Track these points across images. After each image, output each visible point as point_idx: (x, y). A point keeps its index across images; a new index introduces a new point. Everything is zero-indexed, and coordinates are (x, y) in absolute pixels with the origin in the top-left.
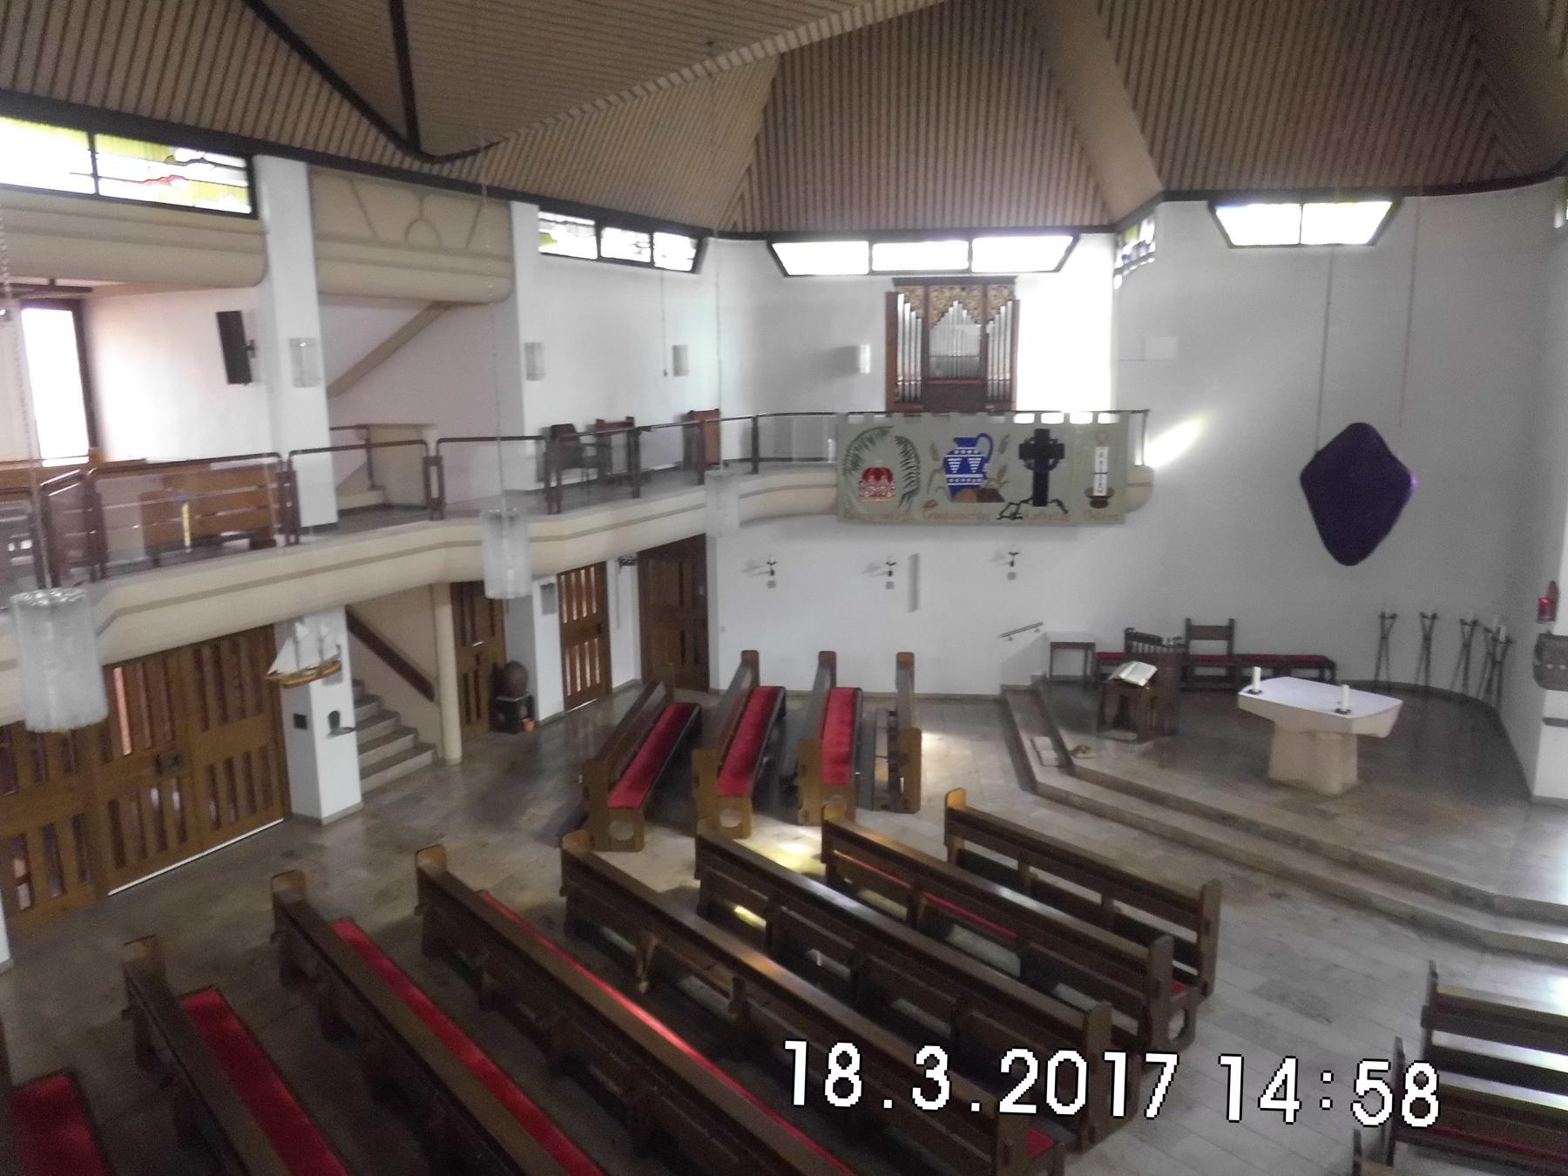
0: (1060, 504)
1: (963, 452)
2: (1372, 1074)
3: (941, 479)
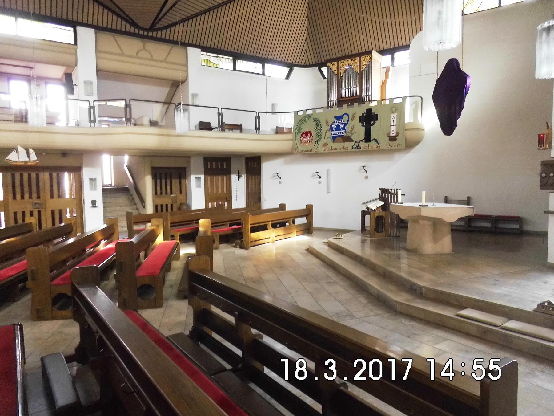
0: (376, 141)
1: (338, 122)
2: (478, 363)
3: (329, 134)
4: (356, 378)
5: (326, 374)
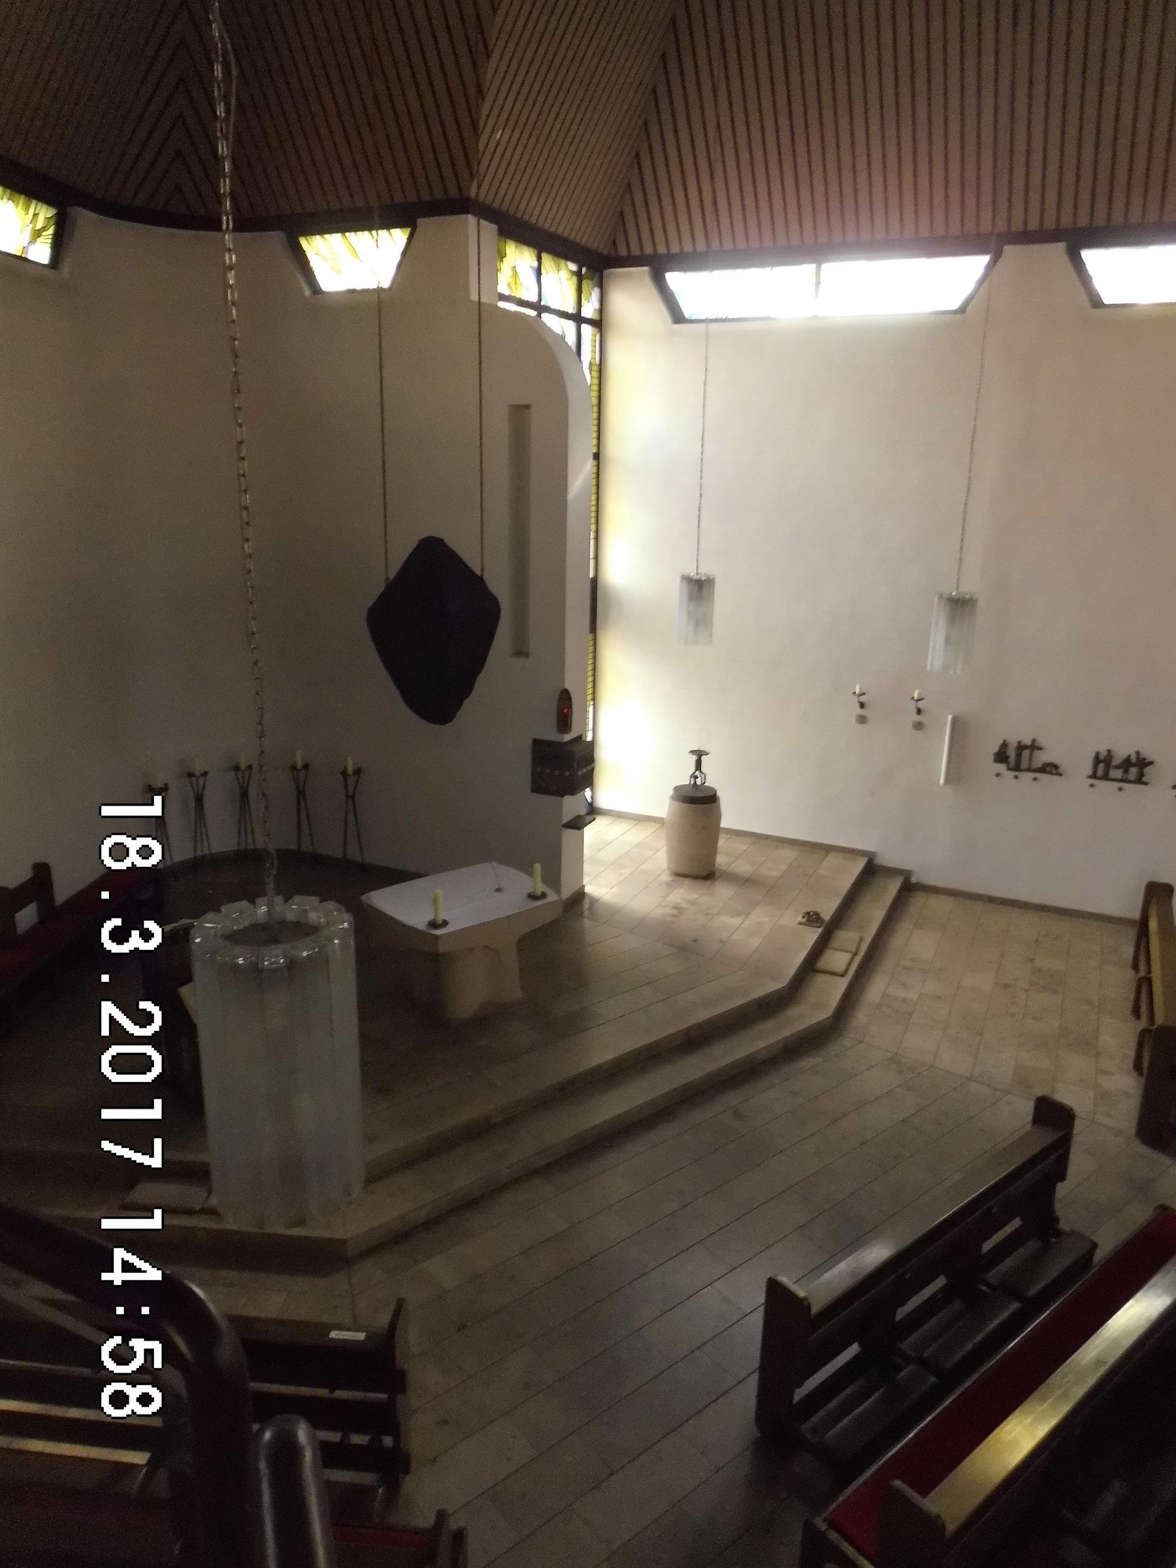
4: (108, 1009)
5: (117, 922)
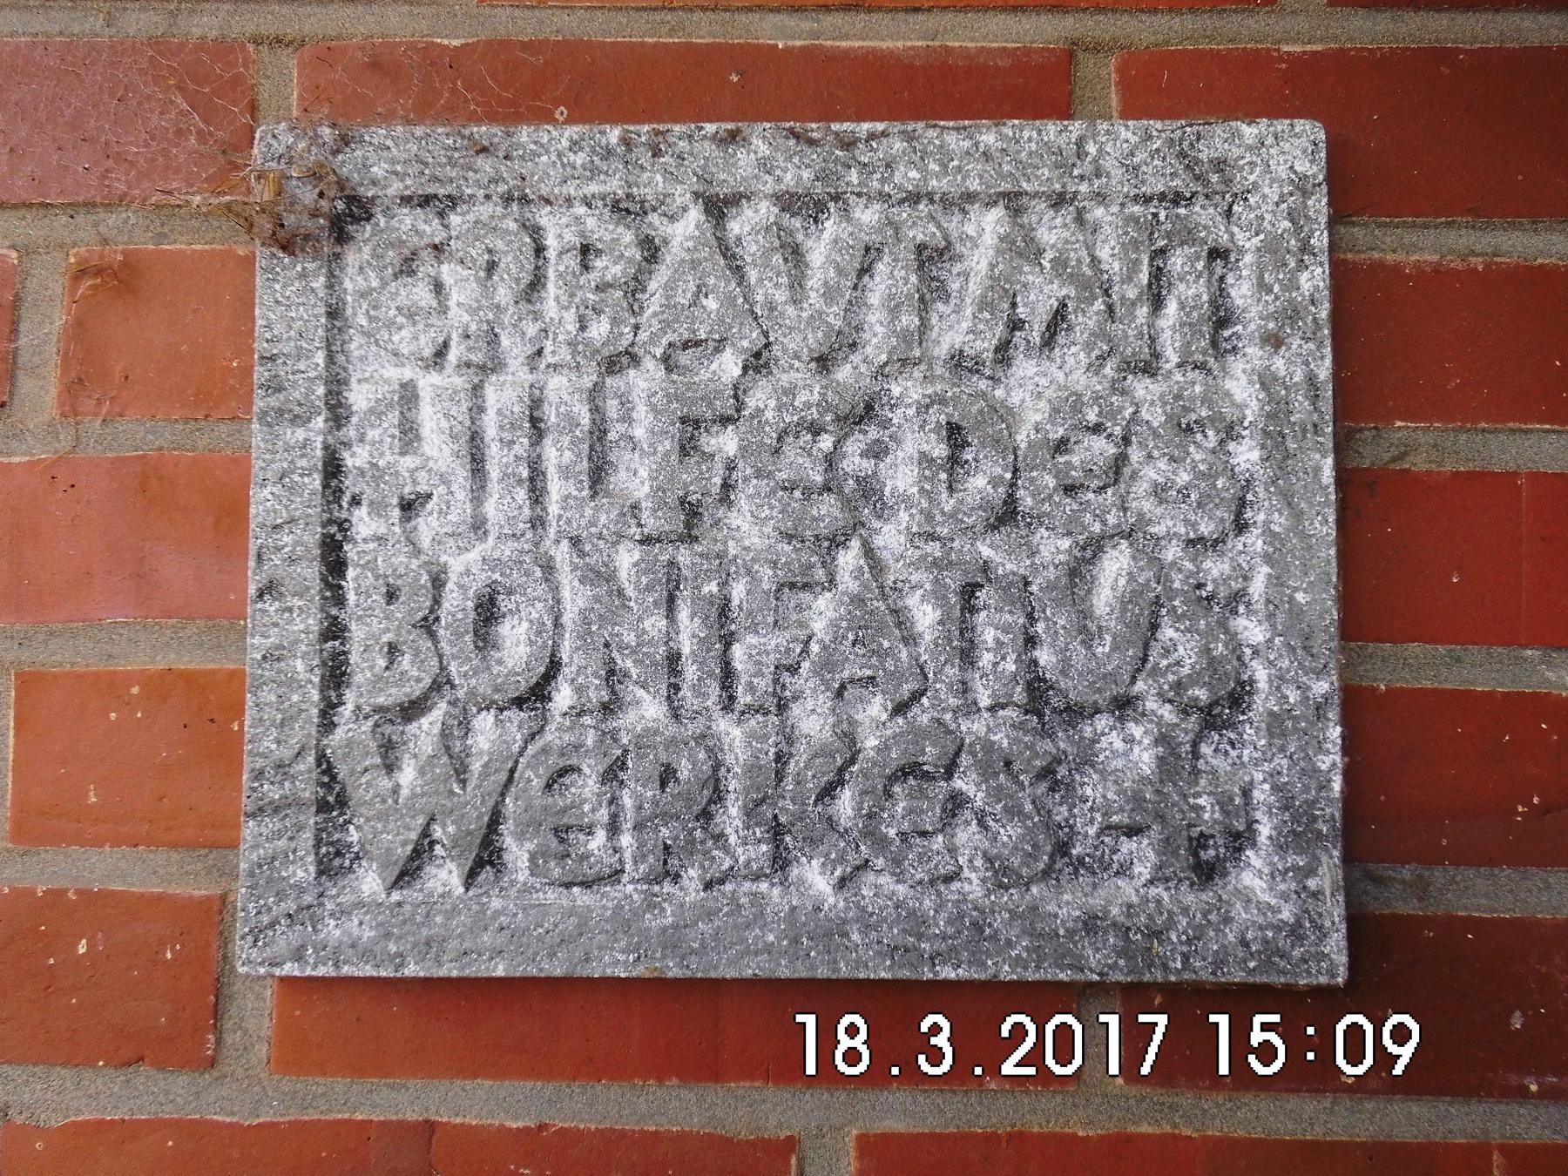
4: (1008, 1068)
5: (922, 1059)
